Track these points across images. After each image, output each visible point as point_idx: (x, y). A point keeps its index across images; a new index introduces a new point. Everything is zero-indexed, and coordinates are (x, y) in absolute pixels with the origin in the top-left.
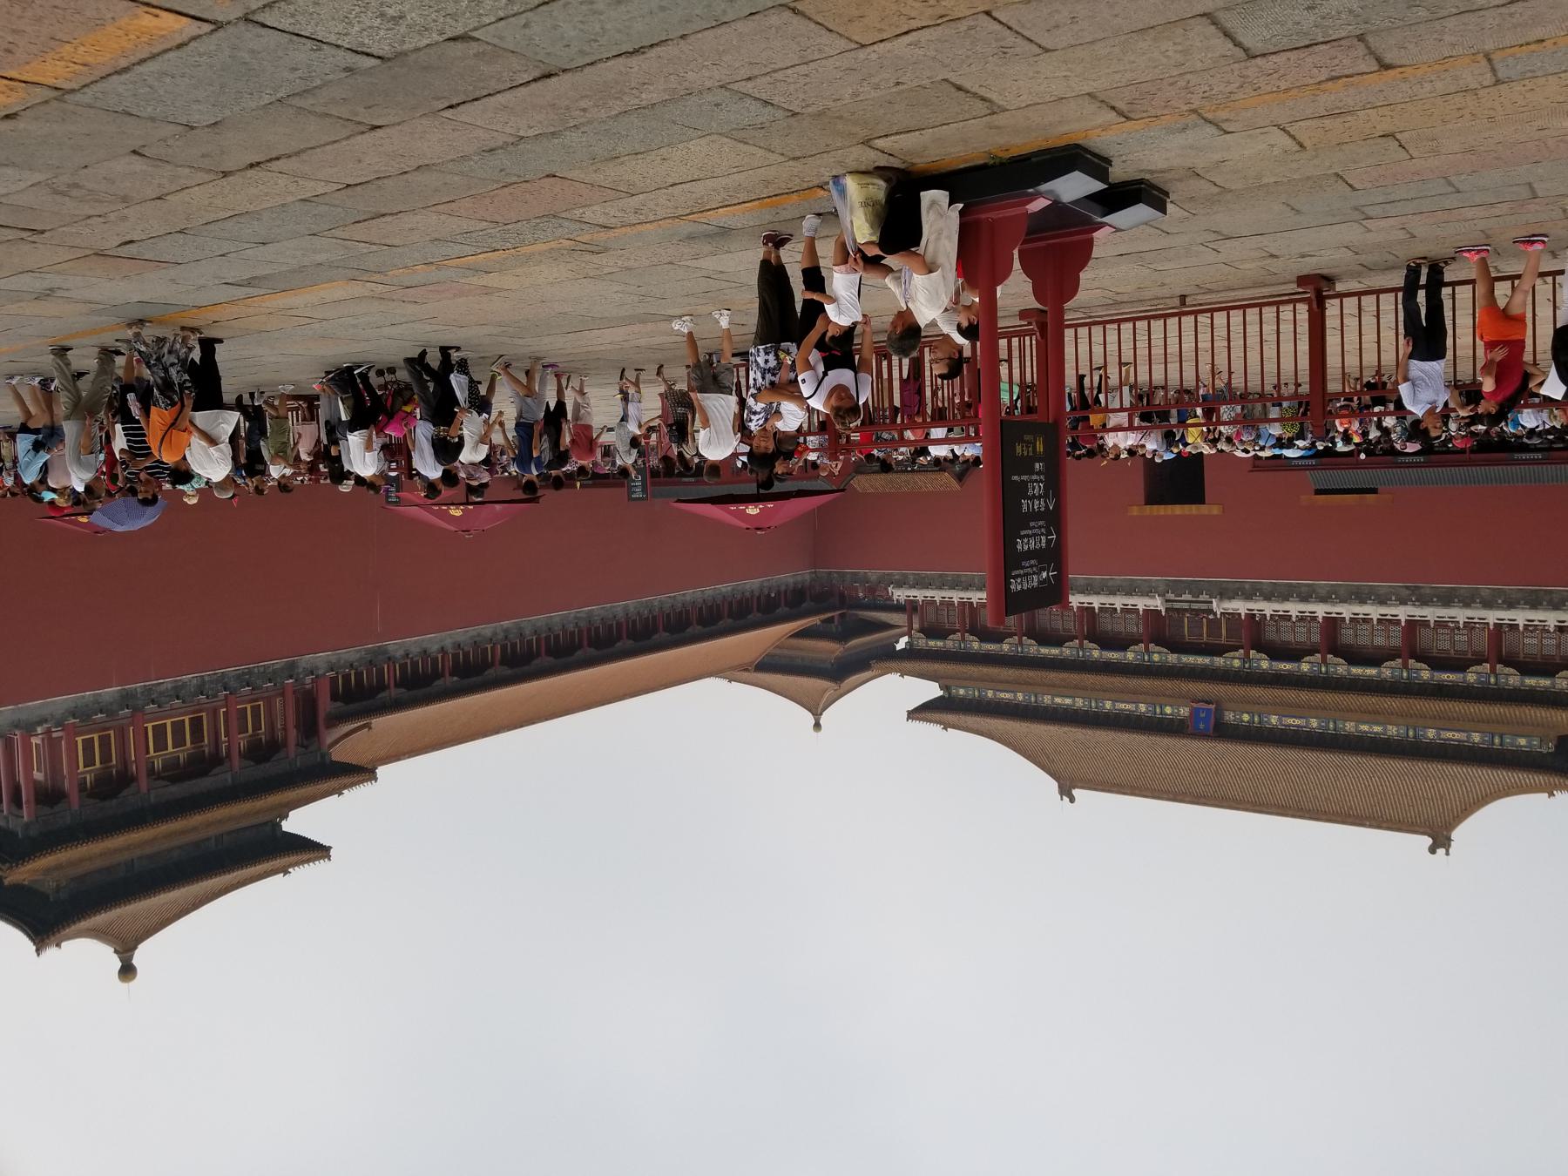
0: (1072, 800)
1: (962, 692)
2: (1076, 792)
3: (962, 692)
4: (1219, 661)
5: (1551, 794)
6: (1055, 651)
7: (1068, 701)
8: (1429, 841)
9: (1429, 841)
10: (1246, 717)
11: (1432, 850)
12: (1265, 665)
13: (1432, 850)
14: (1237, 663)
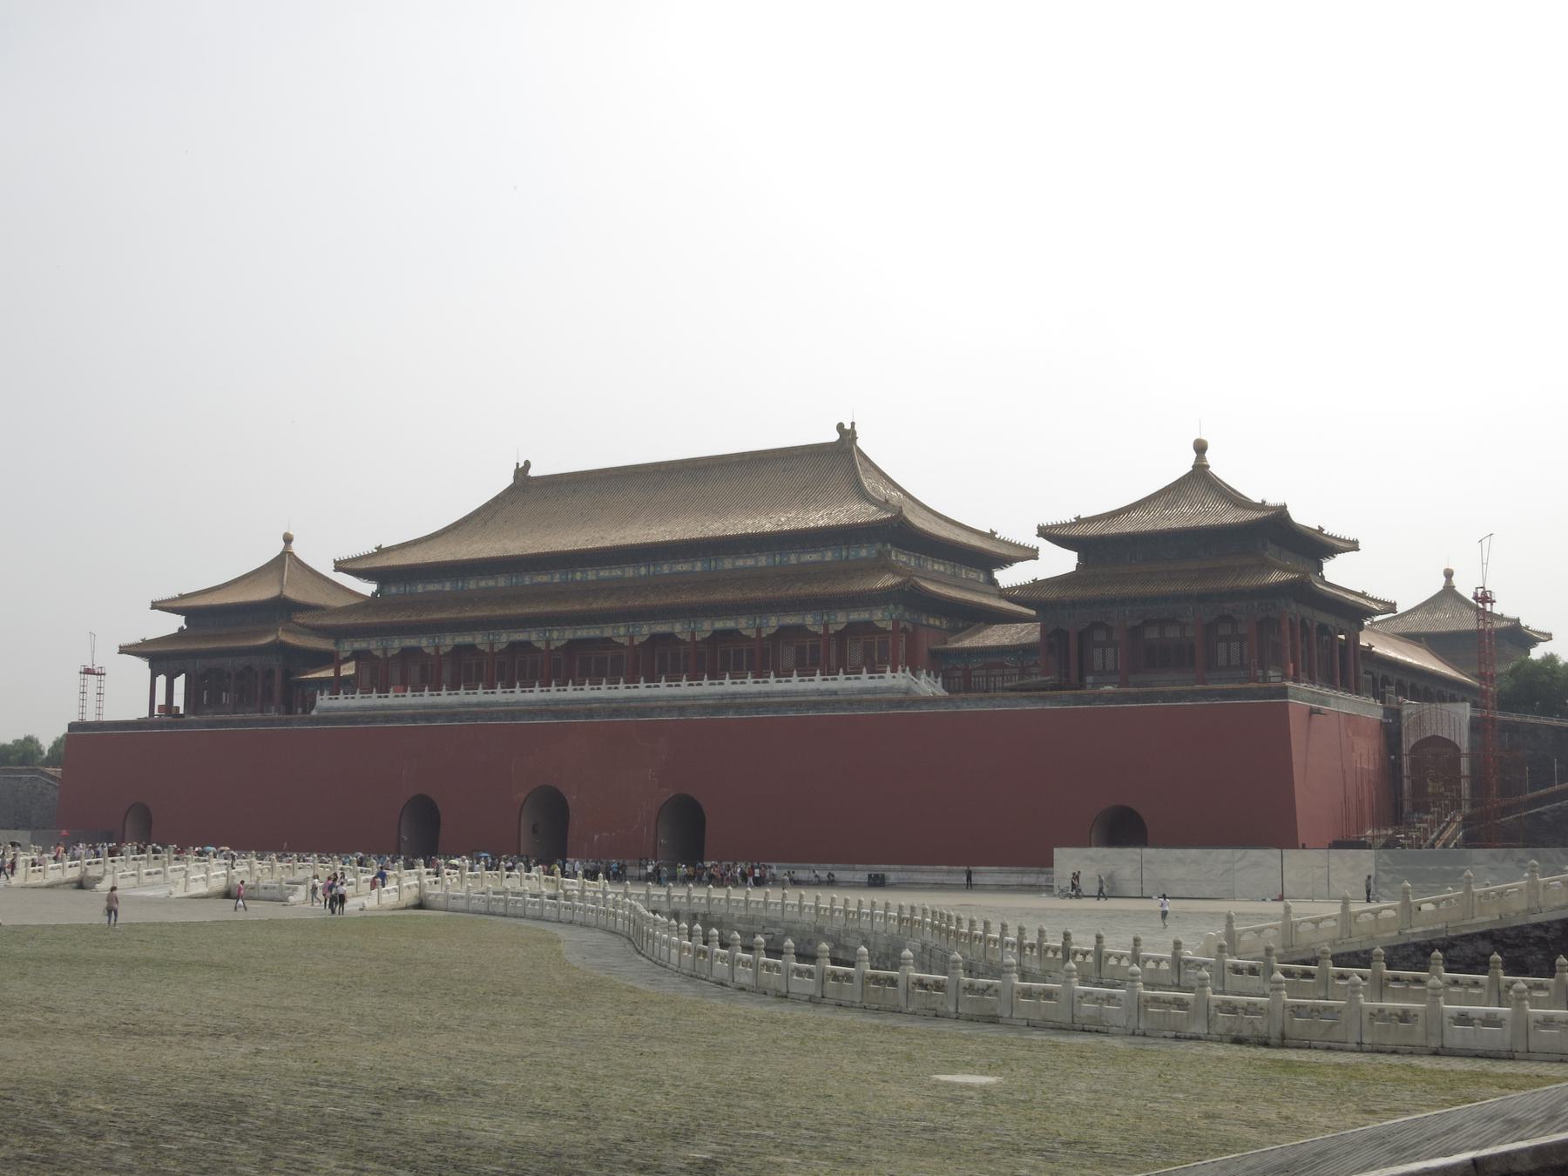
0: (840, 427)
1: (863, 553)
2: (834, 436)
3: (863, 553)
4: (569, 634)
5: (379, 548)
6: (719, 625)
7: (740, 563)
8: (532, 473)
9: (532, 473)
10: (578, 576)
11: (527, 464)
12: (534, 637)
13: (527, 464)
14: (555, 635)
